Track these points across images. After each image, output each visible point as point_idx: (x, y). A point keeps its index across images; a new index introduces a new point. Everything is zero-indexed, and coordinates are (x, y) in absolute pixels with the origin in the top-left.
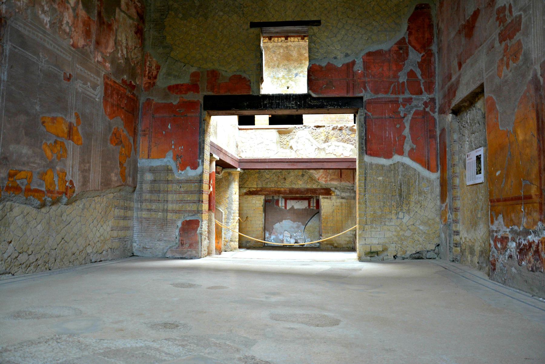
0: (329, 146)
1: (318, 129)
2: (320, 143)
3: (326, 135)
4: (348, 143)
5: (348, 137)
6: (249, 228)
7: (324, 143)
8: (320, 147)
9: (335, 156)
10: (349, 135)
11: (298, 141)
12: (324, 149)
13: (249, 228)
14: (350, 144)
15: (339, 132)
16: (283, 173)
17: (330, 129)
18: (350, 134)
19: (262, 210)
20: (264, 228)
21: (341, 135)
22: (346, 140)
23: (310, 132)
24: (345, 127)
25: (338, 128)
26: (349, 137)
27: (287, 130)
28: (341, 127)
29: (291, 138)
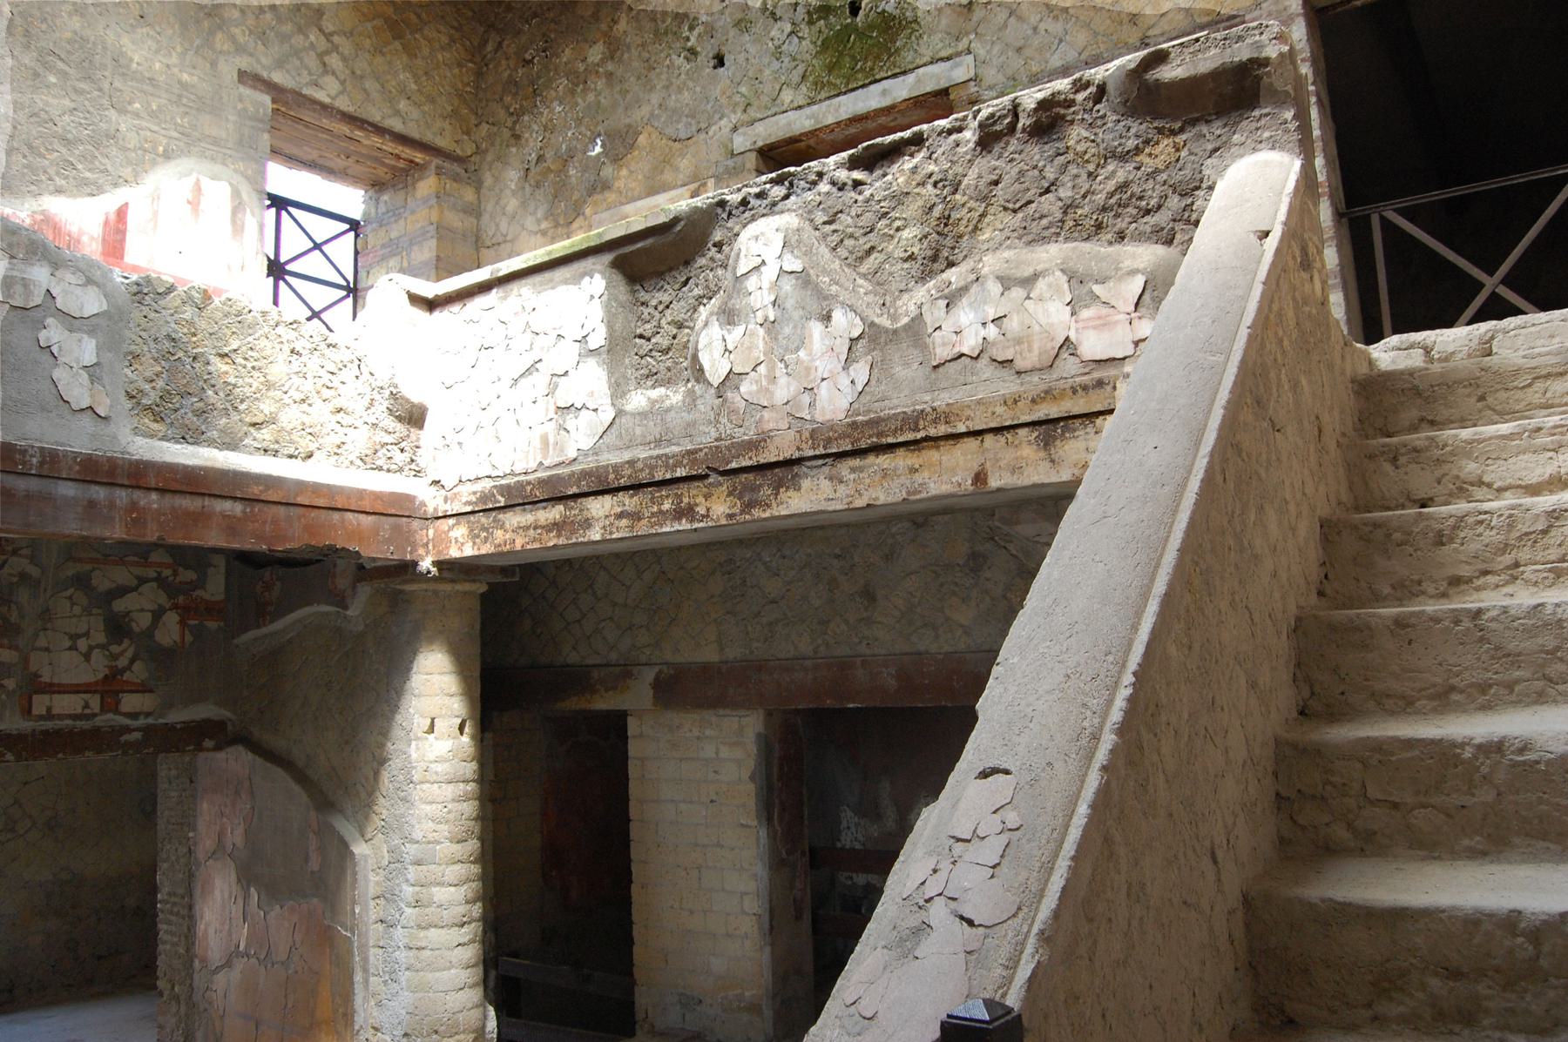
0: (951, 300)
1: (878, 172)
2: (894, 287)
3: (937, 212)
4: (1121, 237)
5: (1121, 176)
6: (692, 912)
7: (922, 278)
8: (885, 322)
9: (1005, 373)
10: (1123, 157)
11: (737, 303)
12: (915, 331)
13: (692, 912)
14: (1140, 237)
15: (1036, 152)
16: (856, 559)
17: (961, 150)
18: (1131, 143)
19: (752, 803)
20: (766, 918)
21: (1050, 174)
22: (1104, 209)
23: (820, 217)
24: (1080, 97)
25: (1020, 125)
26: (1122, 173)
27: (669, 237)
28: (1043, 105)
29: (697, 292)
